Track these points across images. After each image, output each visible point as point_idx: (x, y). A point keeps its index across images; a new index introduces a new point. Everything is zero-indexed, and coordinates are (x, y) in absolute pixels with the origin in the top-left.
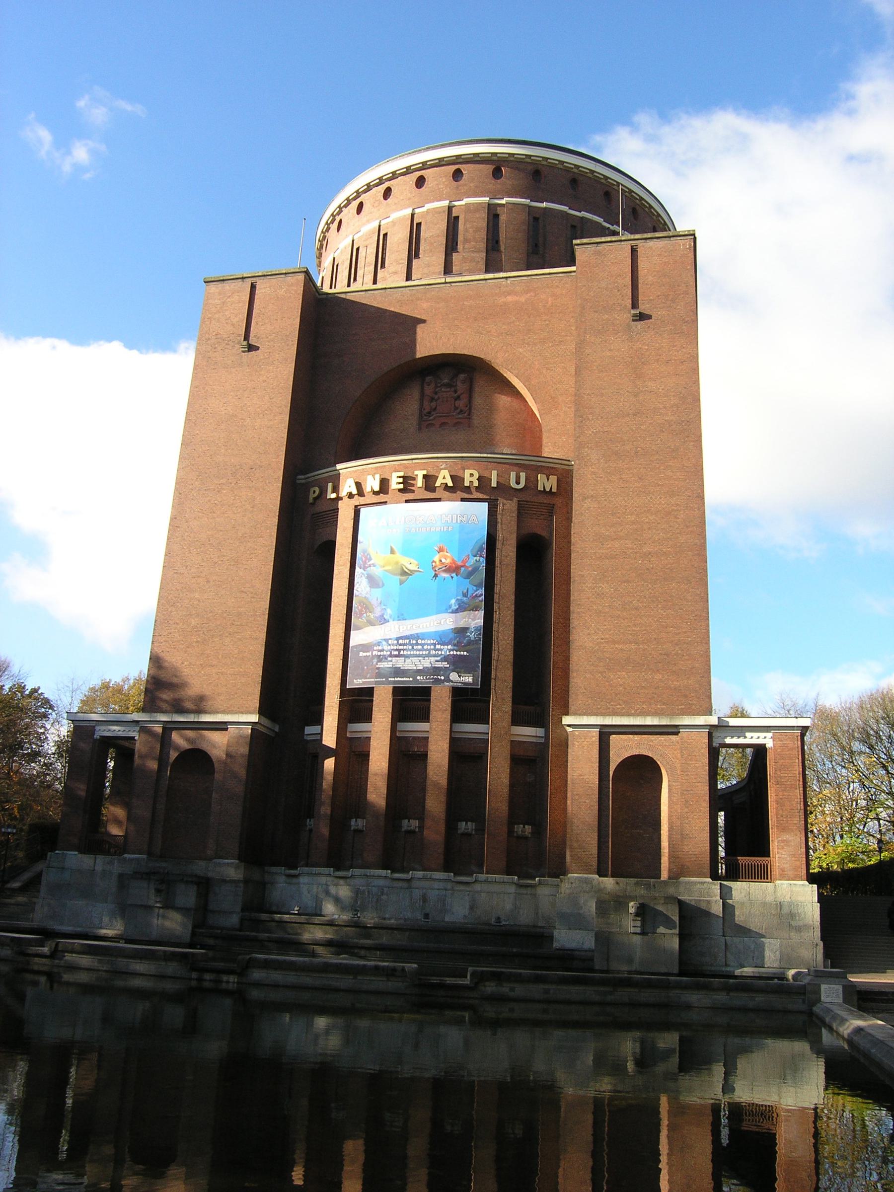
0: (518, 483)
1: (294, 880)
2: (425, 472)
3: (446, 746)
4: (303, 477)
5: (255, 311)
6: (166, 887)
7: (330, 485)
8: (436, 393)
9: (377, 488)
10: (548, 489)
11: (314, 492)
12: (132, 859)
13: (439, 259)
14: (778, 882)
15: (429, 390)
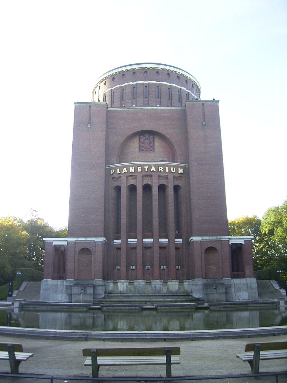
0: (173, 171)
1: (116, 284)
2: (148, 167)
4: (108, 166)
6: (84, 287)
7: (118, 169)
8: (144, 141)
9: (133, 171)
10: (181, 173)
11: (113, 171)
12: (69, 281)
14: (247, 278)
15: (142, 140)
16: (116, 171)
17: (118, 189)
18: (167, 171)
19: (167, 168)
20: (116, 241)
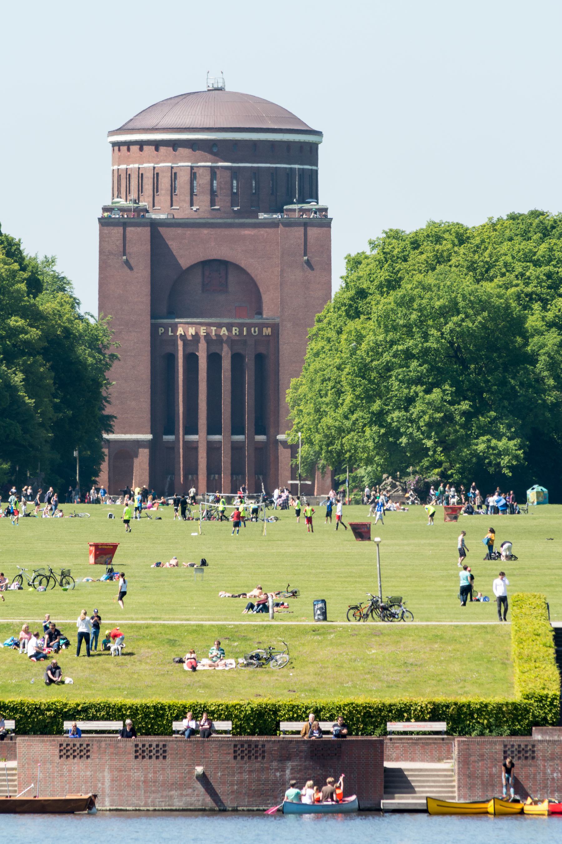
3: (230, 445)
5: (127, 239)
7: (170, 329)
13: (207, 198)
16: (166, 331)
17: (171, 358)
18: (245, 333)
19: (245, 329)
20: (167, 438)
